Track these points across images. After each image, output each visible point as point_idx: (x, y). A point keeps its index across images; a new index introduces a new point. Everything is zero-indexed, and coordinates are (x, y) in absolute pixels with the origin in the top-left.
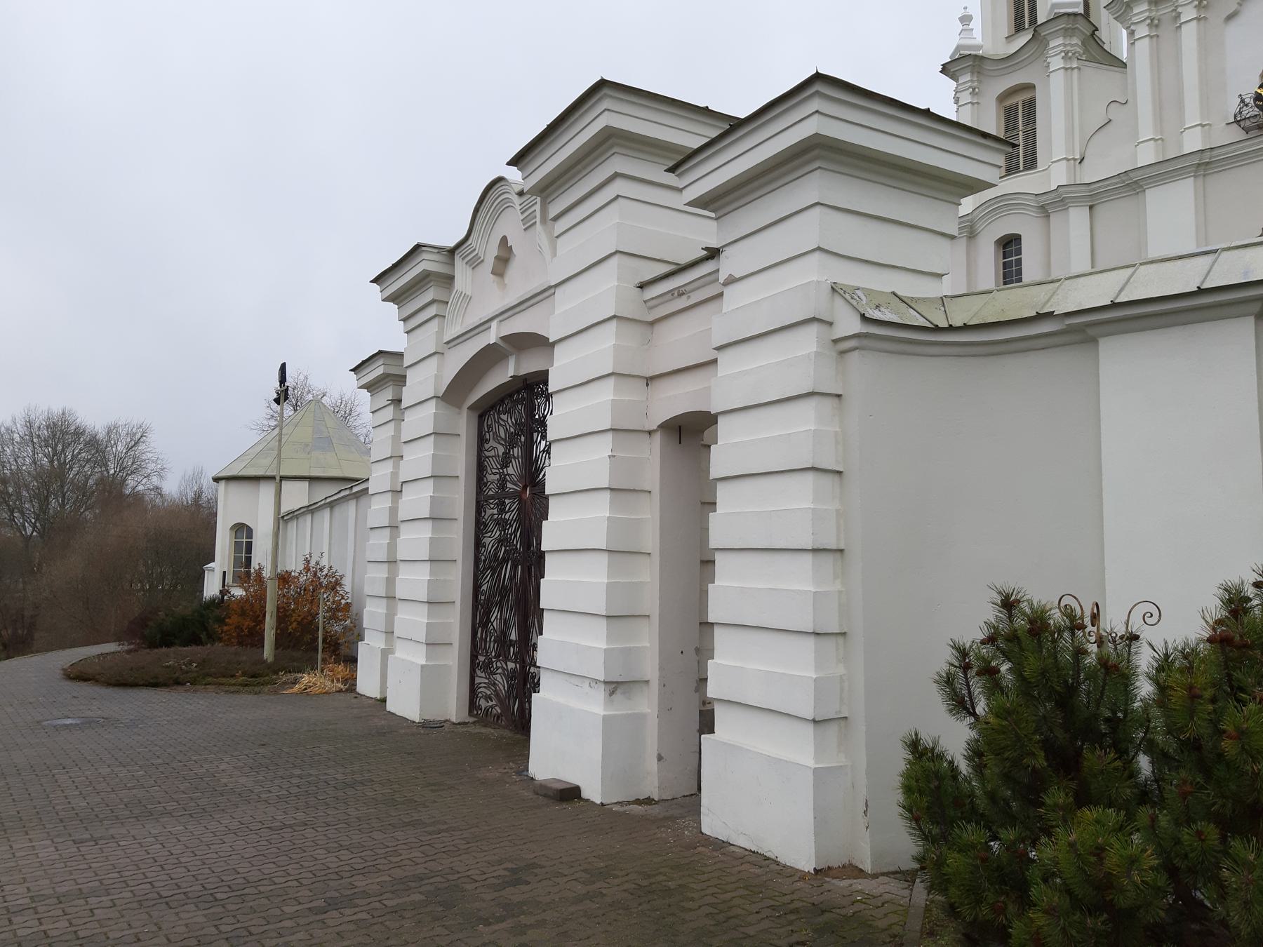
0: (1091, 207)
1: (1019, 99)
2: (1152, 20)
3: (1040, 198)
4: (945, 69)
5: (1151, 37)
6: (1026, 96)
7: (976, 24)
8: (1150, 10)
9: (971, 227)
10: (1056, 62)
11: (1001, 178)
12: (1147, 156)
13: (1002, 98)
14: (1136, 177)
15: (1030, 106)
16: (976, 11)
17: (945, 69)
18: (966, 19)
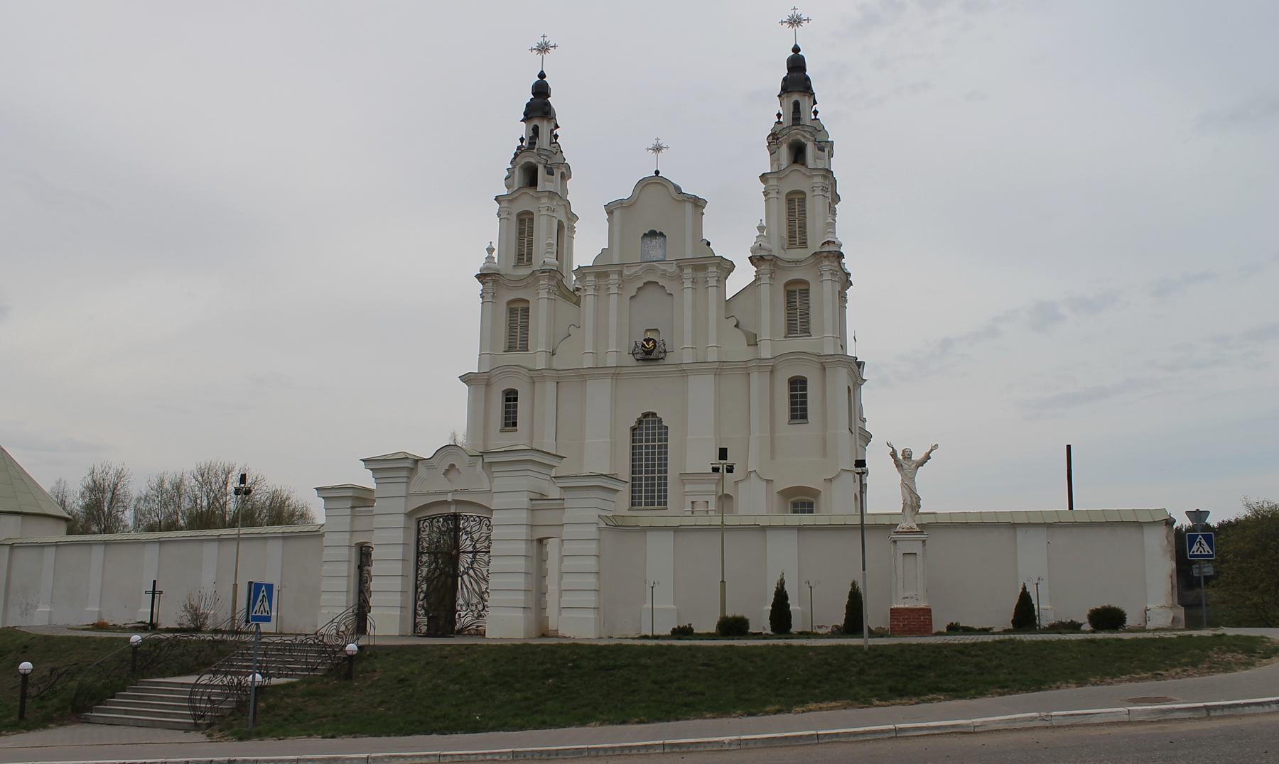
0: (557, 383)
1: (520, 305)
2: (596, 286)
3: (532, 372)
4: (478, 277)
5: (595, 295)
6: (524, 305)
7: (495, 254)
8: (595, 281)
9: (489, 379)
10: (543, 294)
11: (505, 351)
12: (588, 363)
13: (509, 303)
14: (583, 372)
15: (526, 311)
16: (496, 246)
17: (478, 277)
18: (490, 250)
